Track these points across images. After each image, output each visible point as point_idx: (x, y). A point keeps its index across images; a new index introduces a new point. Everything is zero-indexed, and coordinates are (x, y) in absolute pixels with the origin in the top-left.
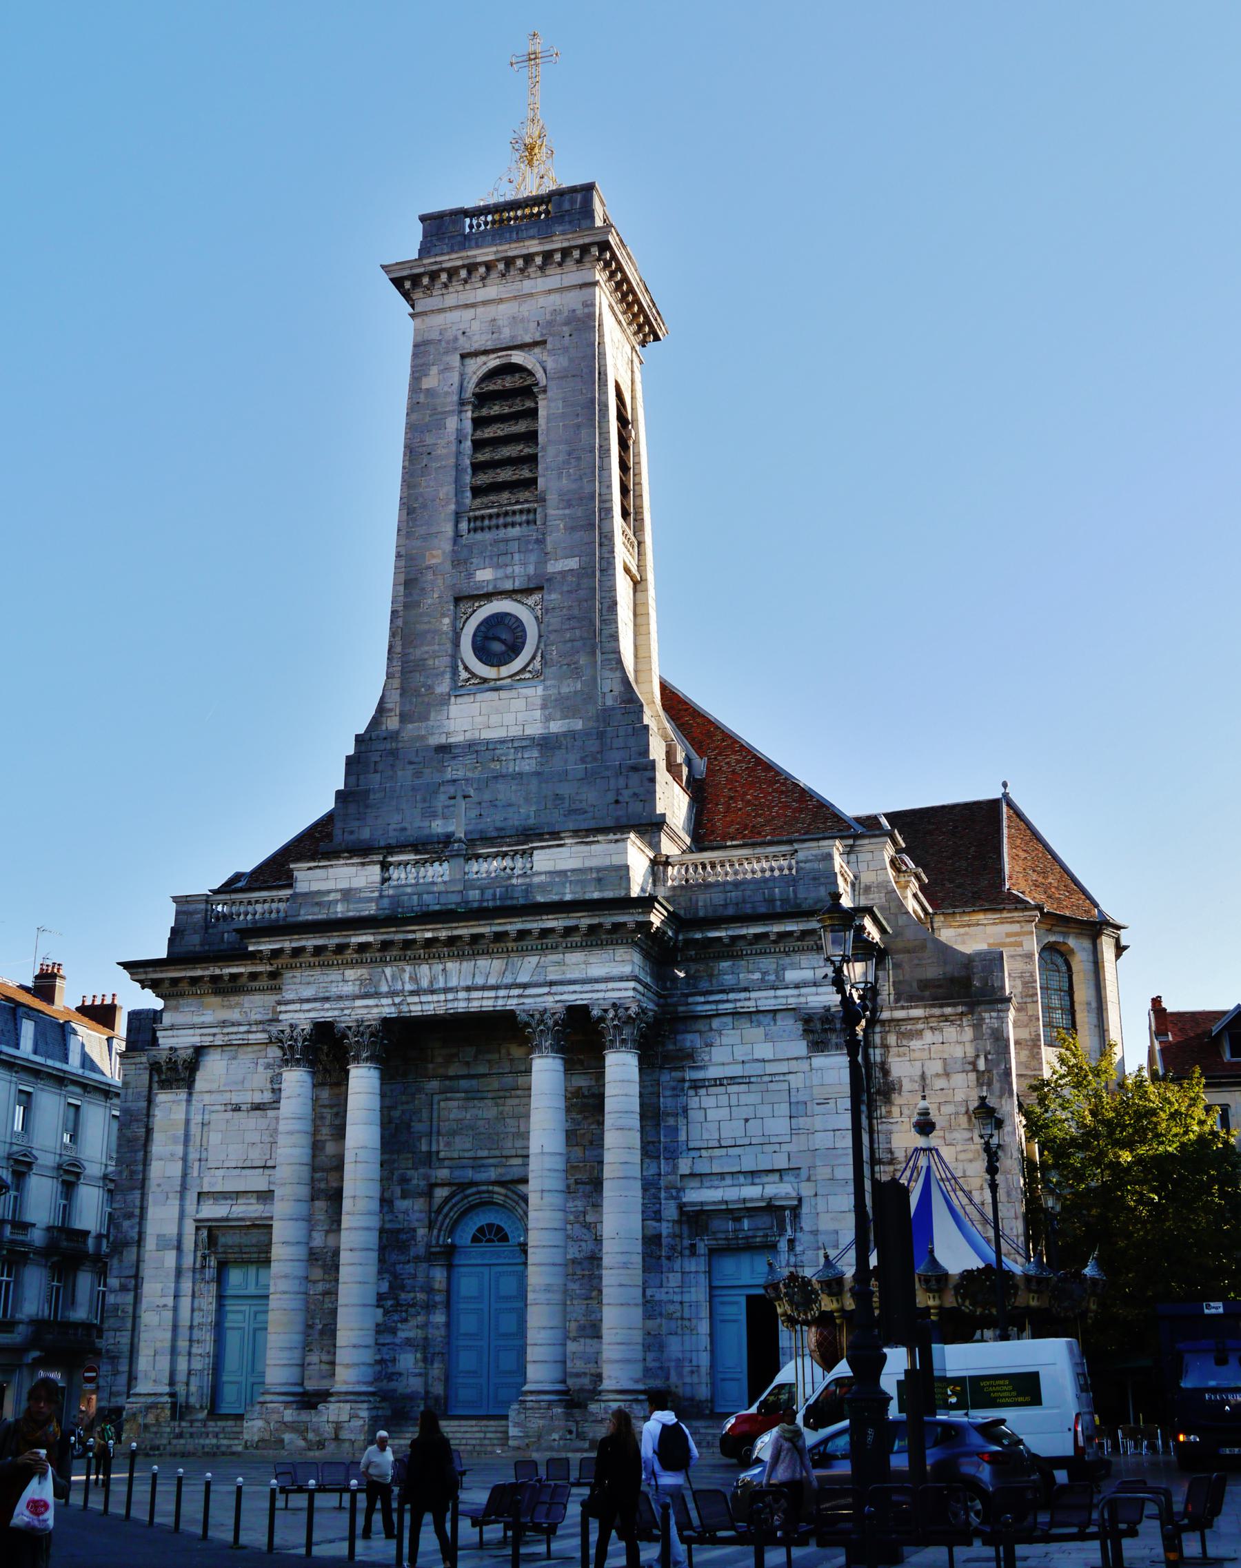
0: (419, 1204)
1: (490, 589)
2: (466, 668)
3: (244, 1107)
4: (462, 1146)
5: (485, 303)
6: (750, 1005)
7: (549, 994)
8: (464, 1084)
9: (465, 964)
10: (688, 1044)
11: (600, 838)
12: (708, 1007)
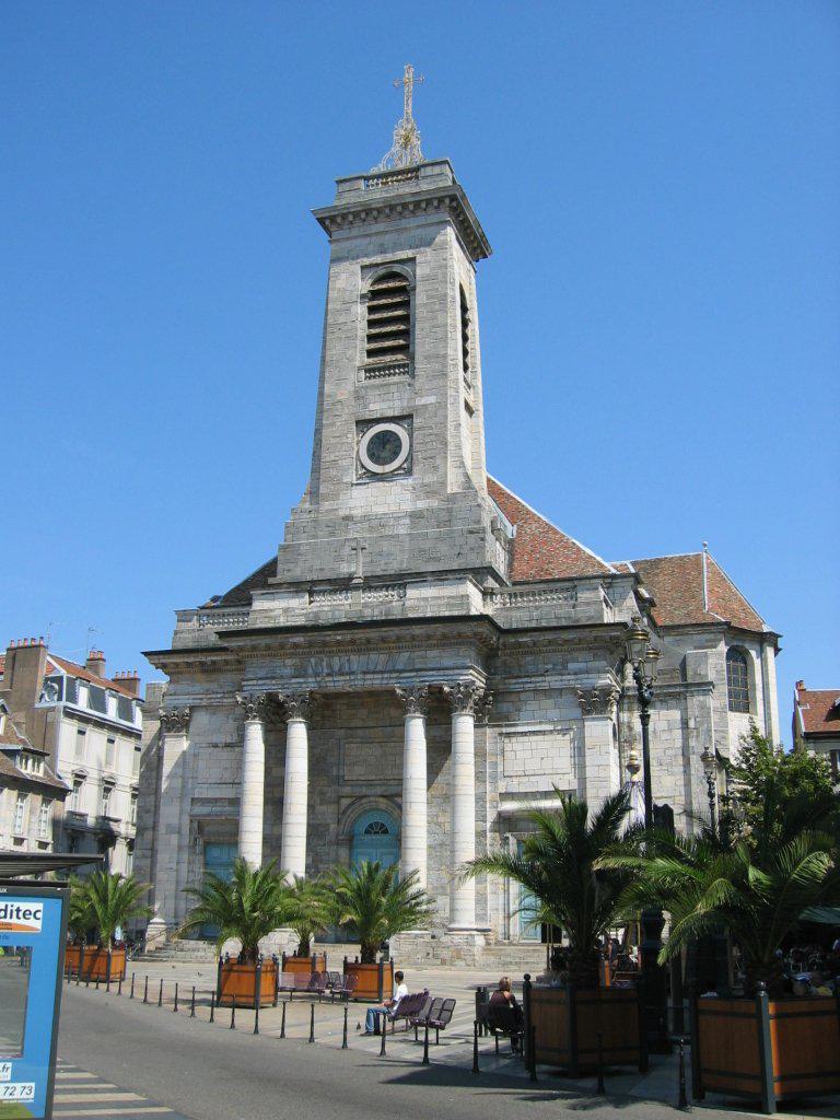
0: (332, 808)
1: (379, 416)
2: (363, 466)
4: (358, 772)
5: (377, 233)
6: (545, 686)
7: (416, 676)
8: (360, 732)
9: (362, 657)
10: (505, 709)
11: (450, 576)
12: (517, 686)
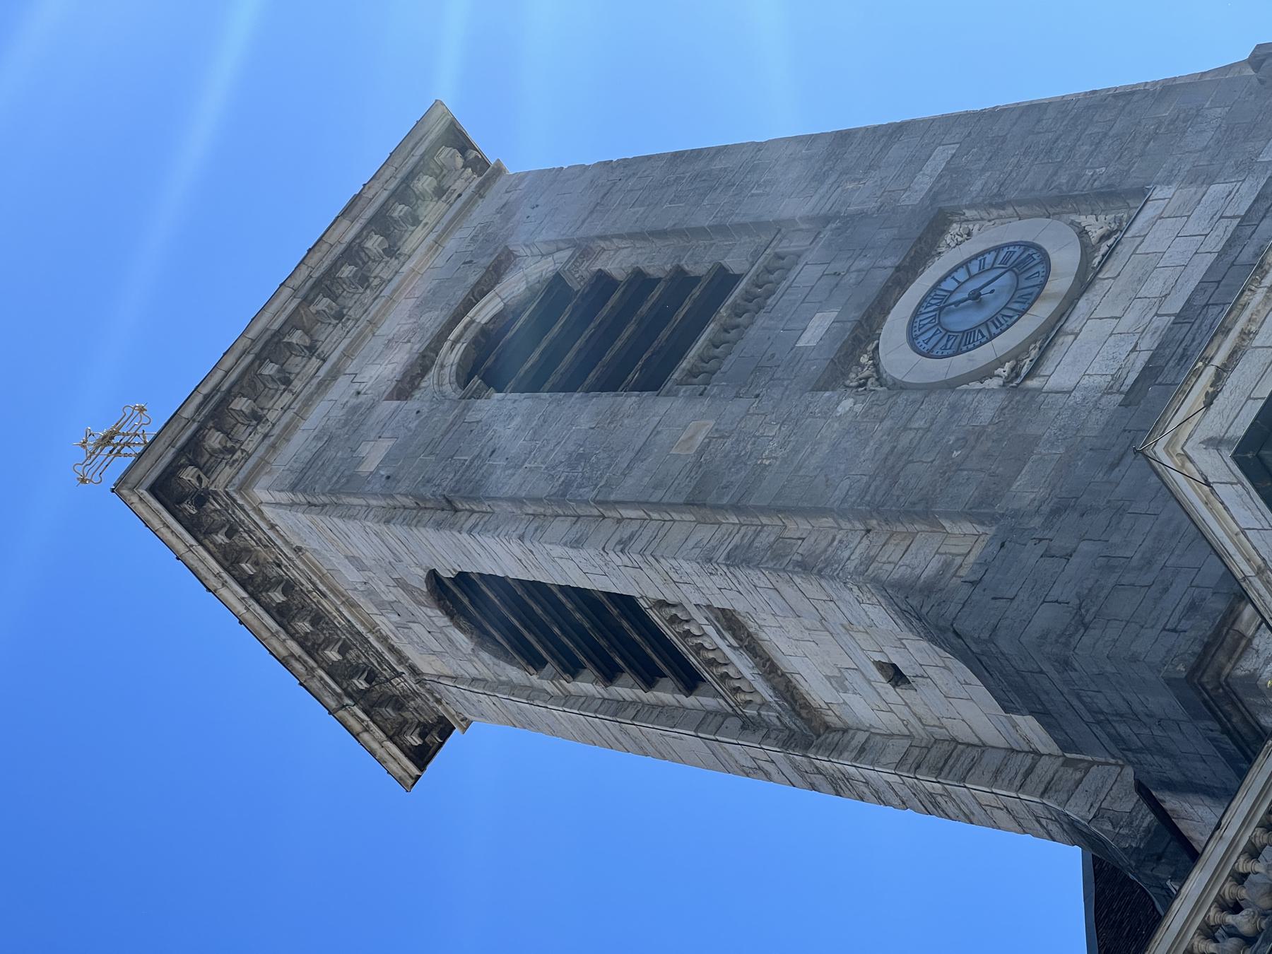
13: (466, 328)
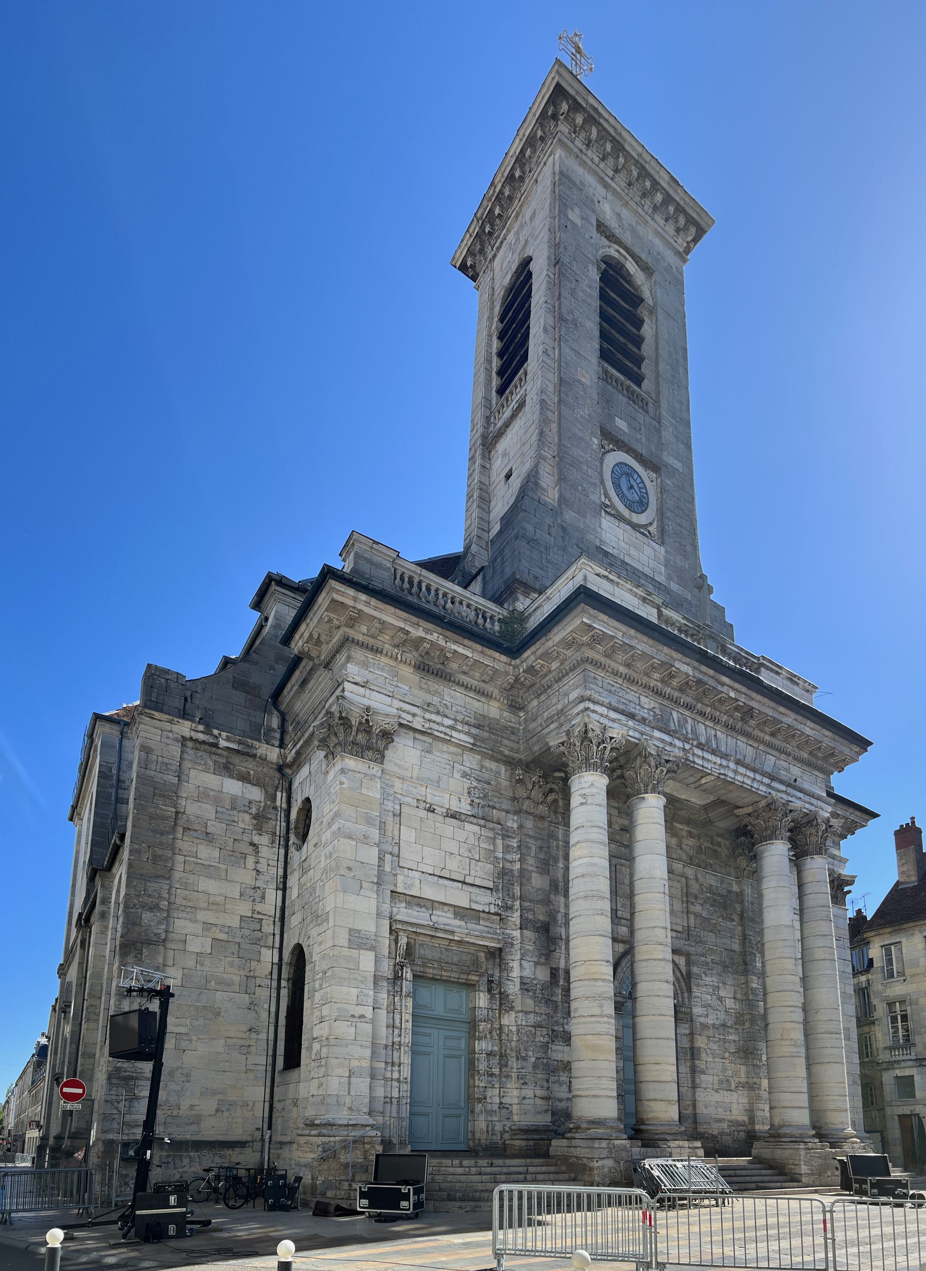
3: (439, 810)
13: (624, 256)
